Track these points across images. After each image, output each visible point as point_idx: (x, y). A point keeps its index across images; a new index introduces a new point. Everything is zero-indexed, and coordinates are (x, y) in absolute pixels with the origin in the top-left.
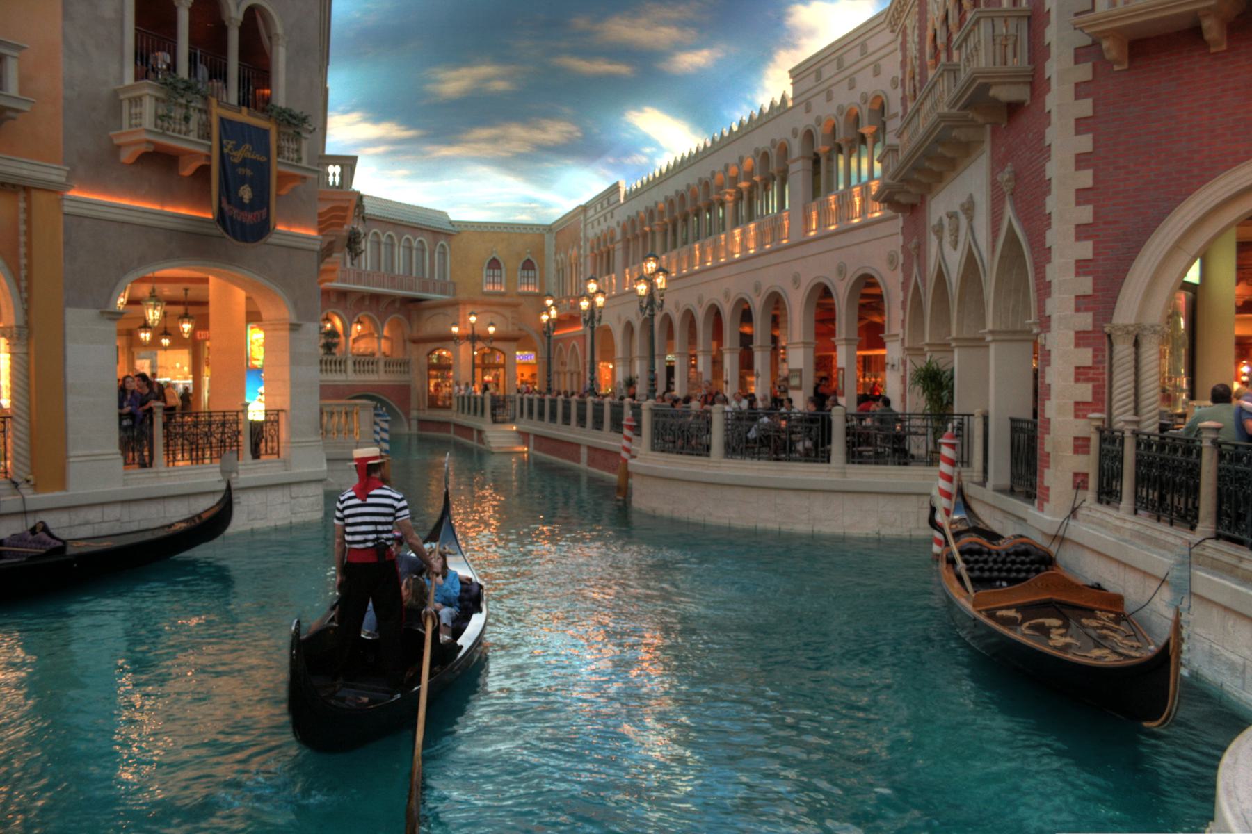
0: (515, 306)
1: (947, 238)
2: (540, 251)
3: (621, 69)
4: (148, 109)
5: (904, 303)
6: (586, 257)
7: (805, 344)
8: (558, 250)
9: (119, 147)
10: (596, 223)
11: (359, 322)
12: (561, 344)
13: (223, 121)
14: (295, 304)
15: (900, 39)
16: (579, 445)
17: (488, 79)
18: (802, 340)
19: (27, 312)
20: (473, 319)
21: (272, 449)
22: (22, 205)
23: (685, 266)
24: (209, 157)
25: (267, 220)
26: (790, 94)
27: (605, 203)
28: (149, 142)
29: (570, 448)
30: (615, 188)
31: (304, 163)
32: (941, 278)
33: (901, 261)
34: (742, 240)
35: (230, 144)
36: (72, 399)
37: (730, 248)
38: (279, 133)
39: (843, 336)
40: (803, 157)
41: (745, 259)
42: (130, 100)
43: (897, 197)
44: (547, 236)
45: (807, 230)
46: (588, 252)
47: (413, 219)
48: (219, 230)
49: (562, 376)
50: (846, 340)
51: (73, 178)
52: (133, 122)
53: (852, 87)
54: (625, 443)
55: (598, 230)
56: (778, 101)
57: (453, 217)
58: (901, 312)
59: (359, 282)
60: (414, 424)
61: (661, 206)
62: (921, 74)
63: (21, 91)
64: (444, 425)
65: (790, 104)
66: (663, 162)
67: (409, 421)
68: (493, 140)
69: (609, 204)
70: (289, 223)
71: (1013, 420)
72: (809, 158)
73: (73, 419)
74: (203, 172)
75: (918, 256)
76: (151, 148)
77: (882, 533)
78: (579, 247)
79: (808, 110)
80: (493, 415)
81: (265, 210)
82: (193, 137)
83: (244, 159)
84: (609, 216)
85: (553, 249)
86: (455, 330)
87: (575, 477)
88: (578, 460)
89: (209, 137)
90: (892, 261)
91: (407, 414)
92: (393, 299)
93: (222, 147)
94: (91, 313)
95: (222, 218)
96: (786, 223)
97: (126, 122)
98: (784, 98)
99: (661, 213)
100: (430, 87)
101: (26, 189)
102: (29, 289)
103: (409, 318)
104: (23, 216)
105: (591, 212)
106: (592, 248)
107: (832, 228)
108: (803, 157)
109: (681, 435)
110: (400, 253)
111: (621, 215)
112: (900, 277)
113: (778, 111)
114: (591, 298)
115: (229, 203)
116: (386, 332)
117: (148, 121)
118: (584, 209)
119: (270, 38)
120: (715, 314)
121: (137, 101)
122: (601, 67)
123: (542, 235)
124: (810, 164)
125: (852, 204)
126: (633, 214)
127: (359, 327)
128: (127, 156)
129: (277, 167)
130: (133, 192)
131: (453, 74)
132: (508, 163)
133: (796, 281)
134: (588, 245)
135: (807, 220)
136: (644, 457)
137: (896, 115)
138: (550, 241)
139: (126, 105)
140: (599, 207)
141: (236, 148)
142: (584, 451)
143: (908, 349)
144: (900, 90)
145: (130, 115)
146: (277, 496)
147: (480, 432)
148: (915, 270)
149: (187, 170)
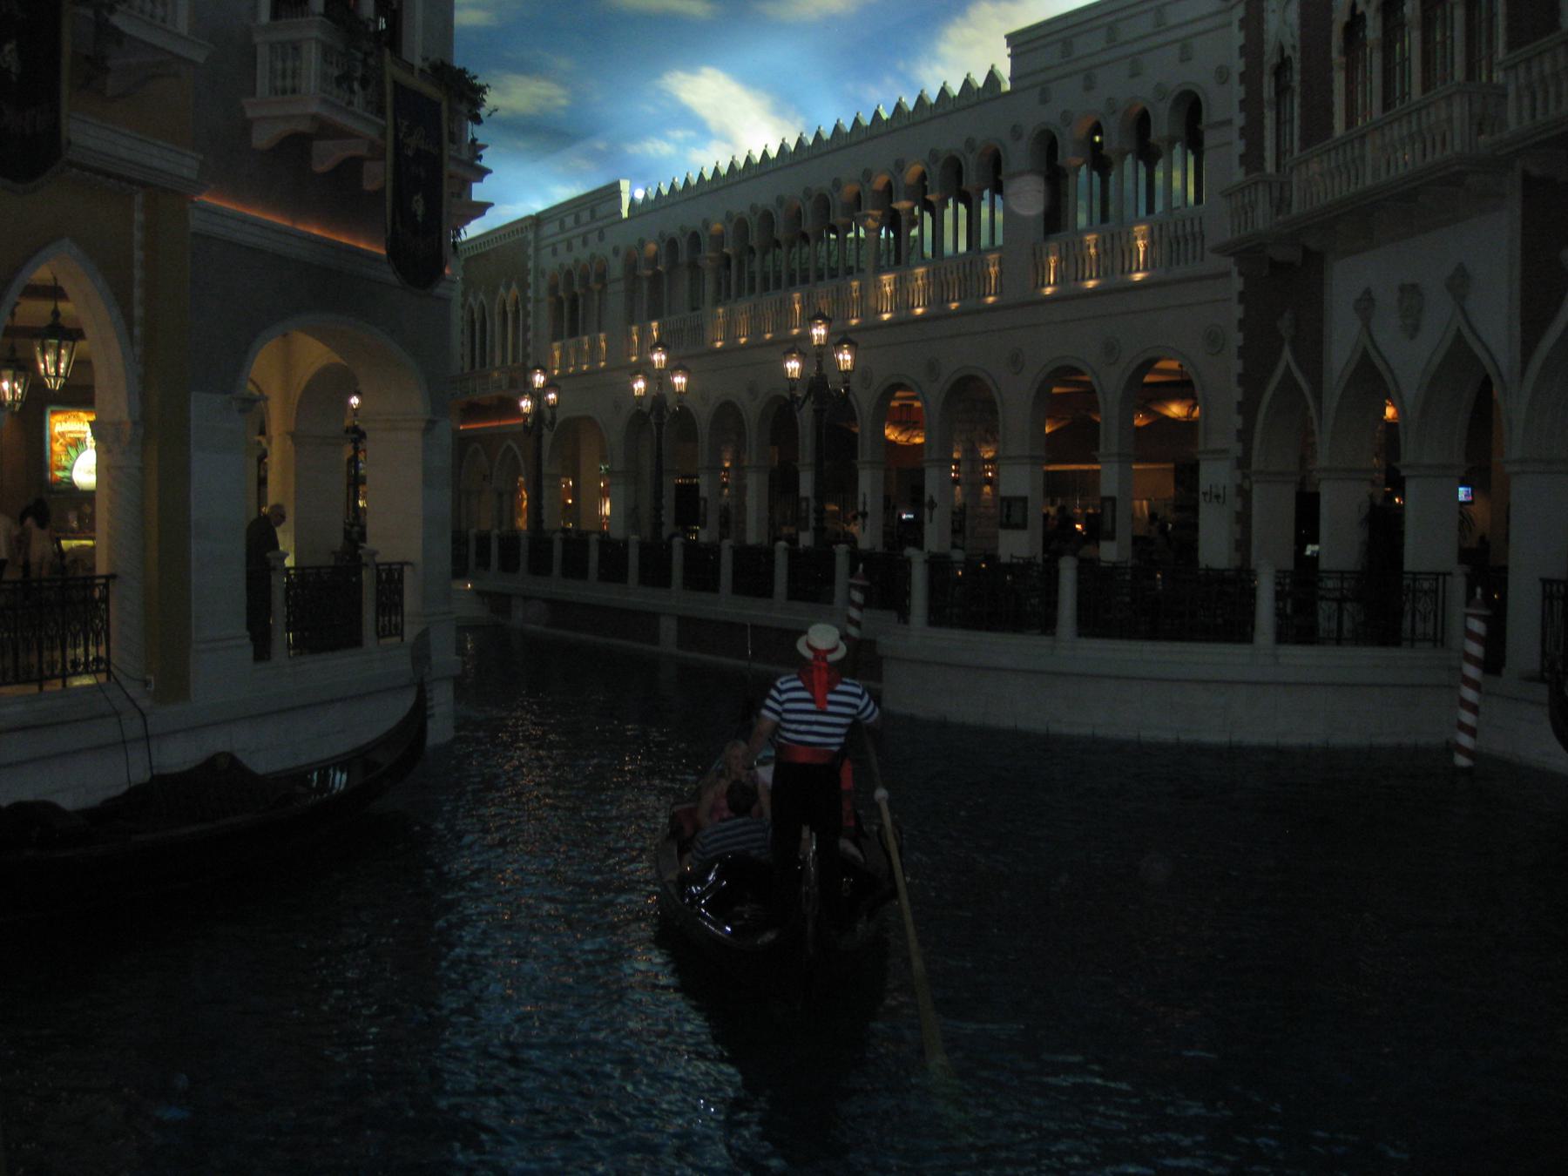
4: (311, 59)
5: (1247, 408)
6: (537, 301)
10: (562, 248)
23: (743, 330)
26: (1005, 70)
27: (585, 216)
28: (314, 117)
34: (895, 291)
37: (872, 303)
41: (904, 322)
52: (279, 83)
54: (854, 613)
55: (568, 260)
56: (979, 80)
58: (1238, 421)
61: (717, 227)
65: (1006, 86)
66: (710, 159)
71: (1545, 582)
74: (350, 169)
78: (524, 286)
79: (1044, 99)
84: (593, 237)
93: (396, 128)
96: (993, 270)
97: (263, 85)
98: (992, 77)
99: (719, 240)
105: (550, 229)
106: (553, 289)
107: (1091, 284)
109: (992, 598)
112: (1237, 366)
113: (978, 98)
125: (1133, 250)
128: (262, 138)
129: (450, 168)
135: (1040, 269)
137: (1229, 122)
140: (570, 221)
142: (668, 628)
144: (1238, 91)
148: (1287, 354)
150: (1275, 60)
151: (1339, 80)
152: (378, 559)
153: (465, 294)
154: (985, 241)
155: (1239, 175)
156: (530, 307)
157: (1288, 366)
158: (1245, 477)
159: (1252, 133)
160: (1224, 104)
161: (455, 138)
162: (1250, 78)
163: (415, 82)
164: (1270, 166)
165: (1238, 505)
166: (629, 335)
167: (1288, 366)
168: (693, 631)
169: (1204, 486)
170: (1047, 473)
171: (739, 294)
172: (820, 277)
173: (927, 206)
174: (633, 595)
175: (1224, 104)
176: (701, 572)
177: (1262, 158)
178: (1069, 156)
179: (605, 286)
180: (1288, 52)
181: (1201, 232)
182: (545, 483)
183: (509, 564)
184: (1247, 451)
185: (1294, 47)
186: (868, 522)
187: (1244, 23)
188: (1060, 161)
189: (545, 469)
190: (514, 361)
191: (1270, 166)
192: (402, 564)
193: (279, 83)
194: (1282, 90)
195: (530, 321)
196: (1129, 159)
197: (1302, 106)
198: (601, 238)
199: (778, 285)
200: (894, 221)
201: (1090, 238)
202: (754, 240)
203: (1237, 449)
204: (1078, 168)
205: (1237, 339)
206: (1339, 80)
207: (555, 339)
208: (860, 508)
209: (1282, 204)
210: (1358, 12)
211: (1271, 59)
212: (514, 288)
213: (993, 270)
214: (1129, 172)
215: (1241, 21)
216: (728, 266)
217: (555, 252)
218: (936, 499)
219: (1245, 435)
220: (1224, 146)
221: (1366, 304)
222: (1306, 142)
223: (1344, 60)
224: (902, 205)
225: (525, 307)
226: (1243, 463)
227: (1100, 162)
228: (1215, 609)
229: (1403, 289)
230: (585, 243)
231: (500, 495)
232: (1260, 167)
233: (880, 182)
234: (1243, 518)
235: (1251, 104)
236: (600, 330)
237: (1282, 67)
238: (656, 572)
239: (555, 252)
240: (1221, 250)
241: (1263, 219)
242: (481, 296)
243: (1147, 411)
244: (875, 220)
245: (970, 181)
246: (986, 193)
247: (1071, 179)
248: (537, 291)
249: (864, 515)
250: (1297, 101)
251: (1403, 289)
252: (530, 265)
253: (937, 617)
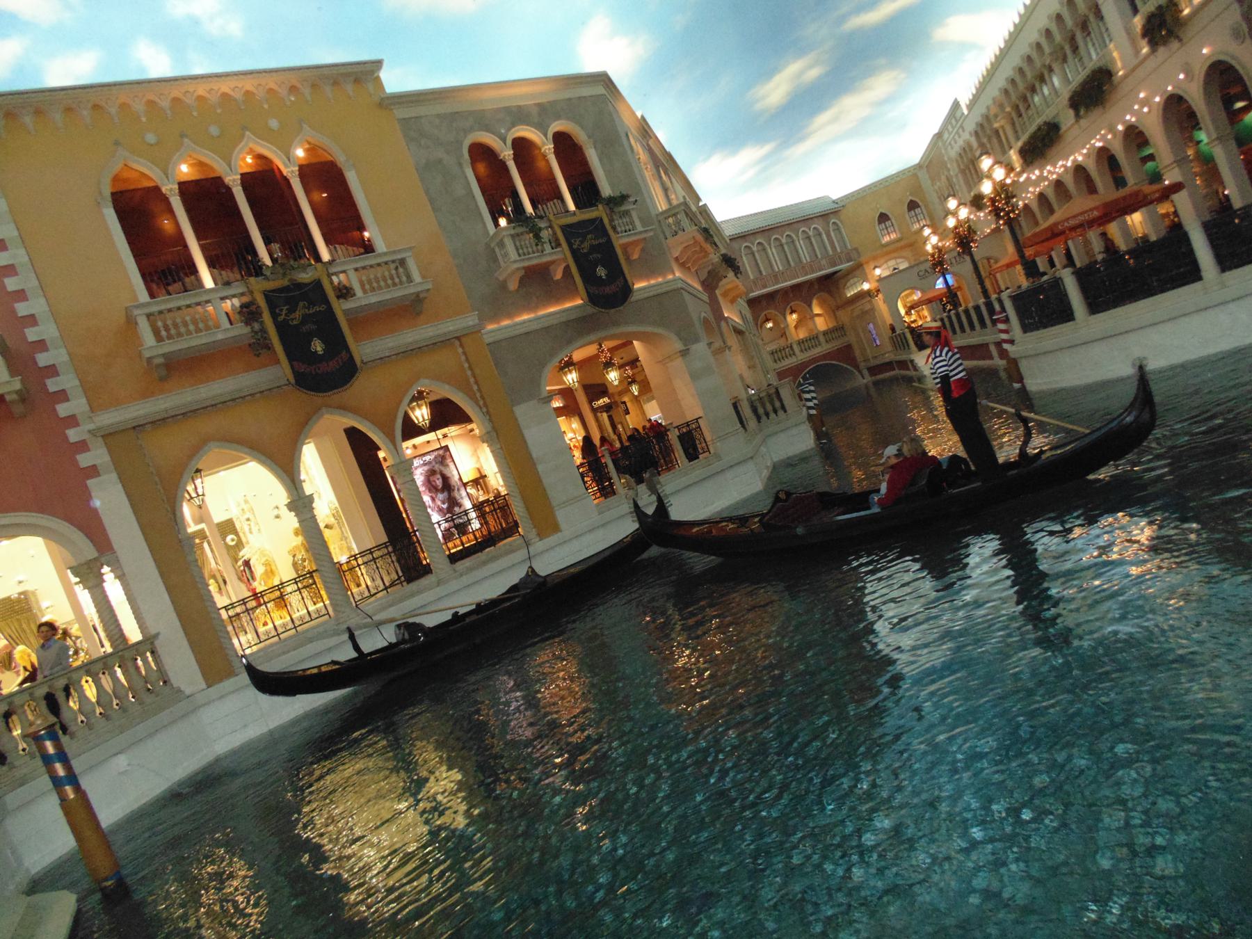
0: (911, 245)
2: (918, 189)
8: (933, 180)
9: (505, 281)
11: (792, 312)
14: (678, 334)
16: (987, 345)
17: (801, 73)
19: (490, 420)
20: (878, 272)
22: (460, 350)
24: (565, 259)
25: (626, 281)
27: (953, 121)
28: (518, 269)
30: (956, 105)
31: (640, 228)
33: (1246, 30)
36: (540, 468)
44: (920, 175)
45: (1137, 51)
47: (799, 215)
51: (484, 319)
57: (834, 198)
59: (777, 283)
60: (865, 372)
63: (423, 277)
64: (889, 366)
67: (860, 372)
68: (835, 120)
69: (957, 121)
70: (642, 277)
73: (547, 481)
76: (522, 273)
78: (949, 170)
80: (916, 344)
83: (592, 246)
86: (866, 286)
88: (991, 358)
89: (559, 245)
91: (857, 367)
92: (810, 283)
94: (533, 403)
95: (593, 299)
96: (1115, 54)
100: (758, 106)
101: (458, 338)
102: (485, 404)
103: (830, 293)
104: (463, 358)
105: (946, 136)
109: (1043, 308)
110: (801, 245)
111: (970, 126)
114: (954, 214)
116: (817, 310)
117: (513, 255)
118: (939, 136)
121: (501, 244)
123: (915, 175)
126: (979, 119)
127: (794, 316)
128: (513, 285)
129: (619, 241)
130: (528, 308)
131: (771, 85)
132: (861, 129)
134: (955, 165)
138: (923, 176)
139: (497, 250)
140: (950, 128)
147: (912, 361)
149: (558, 275)
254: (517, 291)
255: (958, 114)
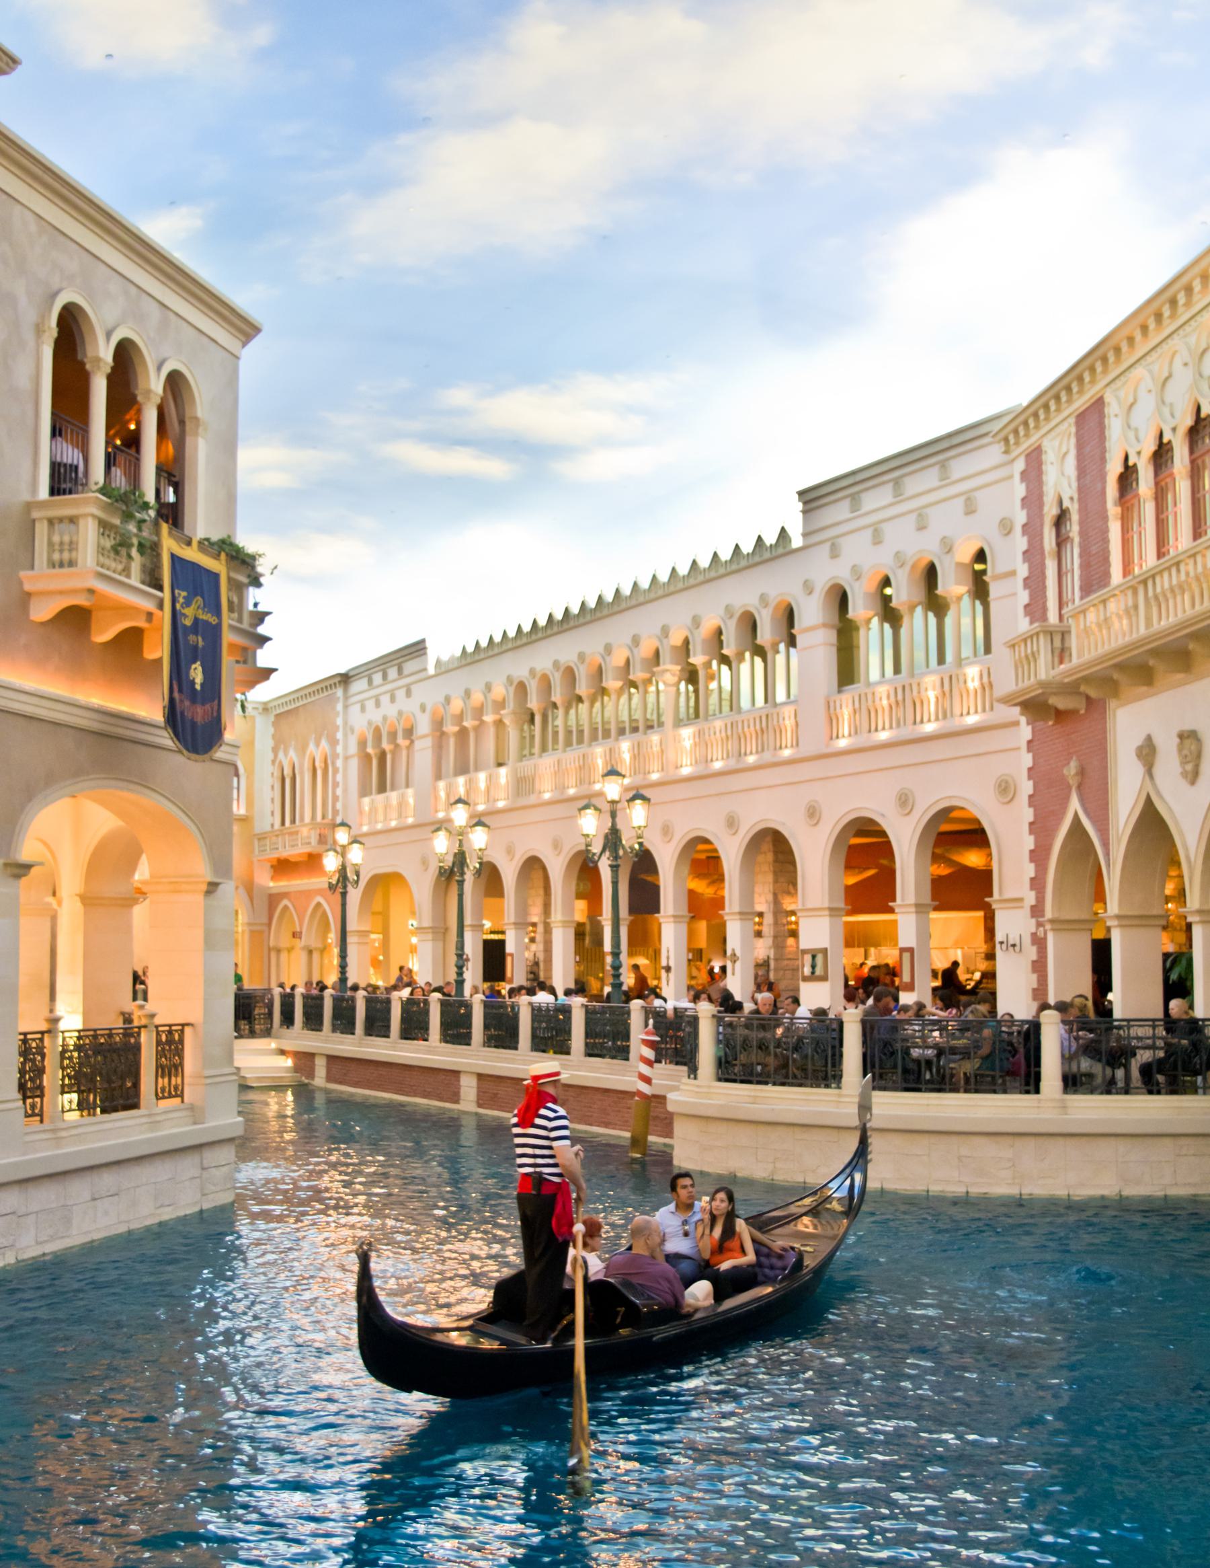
1: (1169, 763)
3: (494, 468)
4: (89, 534)
5: (1039, 856)
6: (346, 758)
7: (833, 912)
9: (29, 595)
12: (285, 902)
13: (174, 557)
15: (1020, 465)
16: (456, 1074)
18: (826, 905)
21: (176, 1088)
28: (91, 591)
29: (444, 1081)
30: (417, 649)
32: (1152, 824)
35: (182, 595)
38: (229, 579)
39: (911, 900)
40: (825, 625)
42: (51, 522)
43: (1052, 701)
45: (833, 736)
46: (353, 749)
48: (166, 739)
49: (284, 955)
50: (917, 905)
52: (56, 556)
53: (921, 528)
54: (645, 1069)
56: (770, 539)
58: (1030, 870)
62: (1081, 523)
72: (832, 627)
74: (131, 639)
75: (1079, 787)
77: (1125, 1193)
78: (333, 742)
81: (216, 702)
82: (135, 581)
83: (196, 620)
84: (401, 694)
85: (271, 743)
87: (450, 1126)
88: (455, 1098)
89: (160, 588)
90: (1005, 789)
93: (174, 600)
106: (362, 744)
108: (825, 625)
112: (1028, 814)
115: (180, 691)
119: (182, 422)
120: (703, 861)
122: (461, 462)
124: (832, 636)
128: (42, 611)
133: (813, 813)
135: (832, 720)
136: (695, 1092)
137: (1013, 573)
139: (41, 529)
141: (188, 603)
142: (469, 1088)
143: (1052, 921)
144: (1022, 543)
145: (50, 544)
146: (187, 1166)
148: (1075, 804)
149: (103, 635)
150: (1055, 511)
151: (1115, 529)
152: (157, 1021)
153: (275, 750)
154: (781, 696)
155: (1024, 625)
156: (339, 763)
157: (1076, 814)
158: (1039, 925)
159: (1035, 583)
160: (1009, 558)
161: (237, 607)
162: (1032, 530)
163: (192, 554)
164: (1053, 617)
165: (1032, 953)
166: (435, 789)
167: (1076, 814)
168: (491, 1086)
169: (999, 936)
170: (847, 923)
171: (544, 749)
172: (621, 732)
173: (725, 660)
174: (431, 1052)
175: (1009, 558)
176: (502, 1032)
177: (1045, 609)
178: (859, 609)
179: (412, 742)
180: (1066, 503)
181: (990, 683)
182: (350, 939)
183: (313, 1020)
184: (1040, 899)
185: (1072, 499)
186: (672, 975)
187: (1024, 475)
188: (851, 614)
189: (352, 926)
190: (323, 817)
191: (1053, 617)
192: (183, 1025)
193: (56, 556)
194: (1061, 541)
195: (339, 777)
196: (919, 610)
197: (1081, 556)
198: (409, 693)
199: (580, 741)
200: (692, 676)
201: (882, 690)
202: (557, 697)
203: (1030, 898)
204: (868, 621)
205: (1027, 787)
206: (1115, 529)
207: (364, 791)
208: (664, 963)
209: (1062, 654)
210: (1131, 463)
211: (1050, 511)
212: (324, 743)
213: (789, 723)
214: (919, 623)
215: (1023, 473)
216: (532, 720)
217: (363, 709)
218: (738, 953)
219: (1037, 884)
220: (1009, 598)
221: (1147, 753)
222: (1087, 589)
223: (1119, 510)
224: (697, 659)
225: (333, 763)
226: (1037, 911)
227: (890, 615)
228: (1010, 1062)
229: (1182, 736)
230: (393, 699)
231: (310, 952)
232: (1044, 617)
233: (676, 639)
234: (1039, 966)
235: (1033, 555)
236: (407, 786)
237: (1061, 520)
238: (456, 1029)
239: (363, 709)
240: (1007, 700)
241: (1045, 670)
242: (292, 754)
243: (950, 862)
244: (674, 675)
245: (765, 635)
246: (747, 655)
247: (862, 632)
248: (345, 748)
249: (668, 969)
250: (1076, 551)
251: (1182, 736)
252: (339, 721)
253: (727, 1070)
254: (43, 624)
255: (410, 667)
